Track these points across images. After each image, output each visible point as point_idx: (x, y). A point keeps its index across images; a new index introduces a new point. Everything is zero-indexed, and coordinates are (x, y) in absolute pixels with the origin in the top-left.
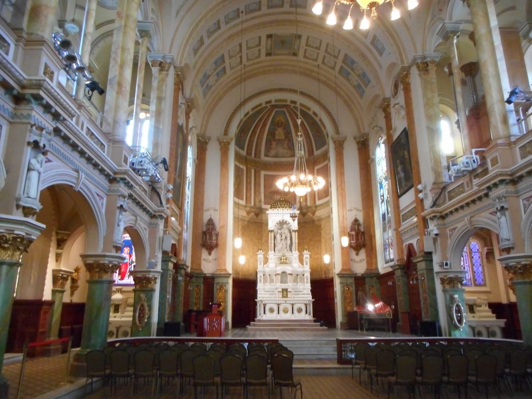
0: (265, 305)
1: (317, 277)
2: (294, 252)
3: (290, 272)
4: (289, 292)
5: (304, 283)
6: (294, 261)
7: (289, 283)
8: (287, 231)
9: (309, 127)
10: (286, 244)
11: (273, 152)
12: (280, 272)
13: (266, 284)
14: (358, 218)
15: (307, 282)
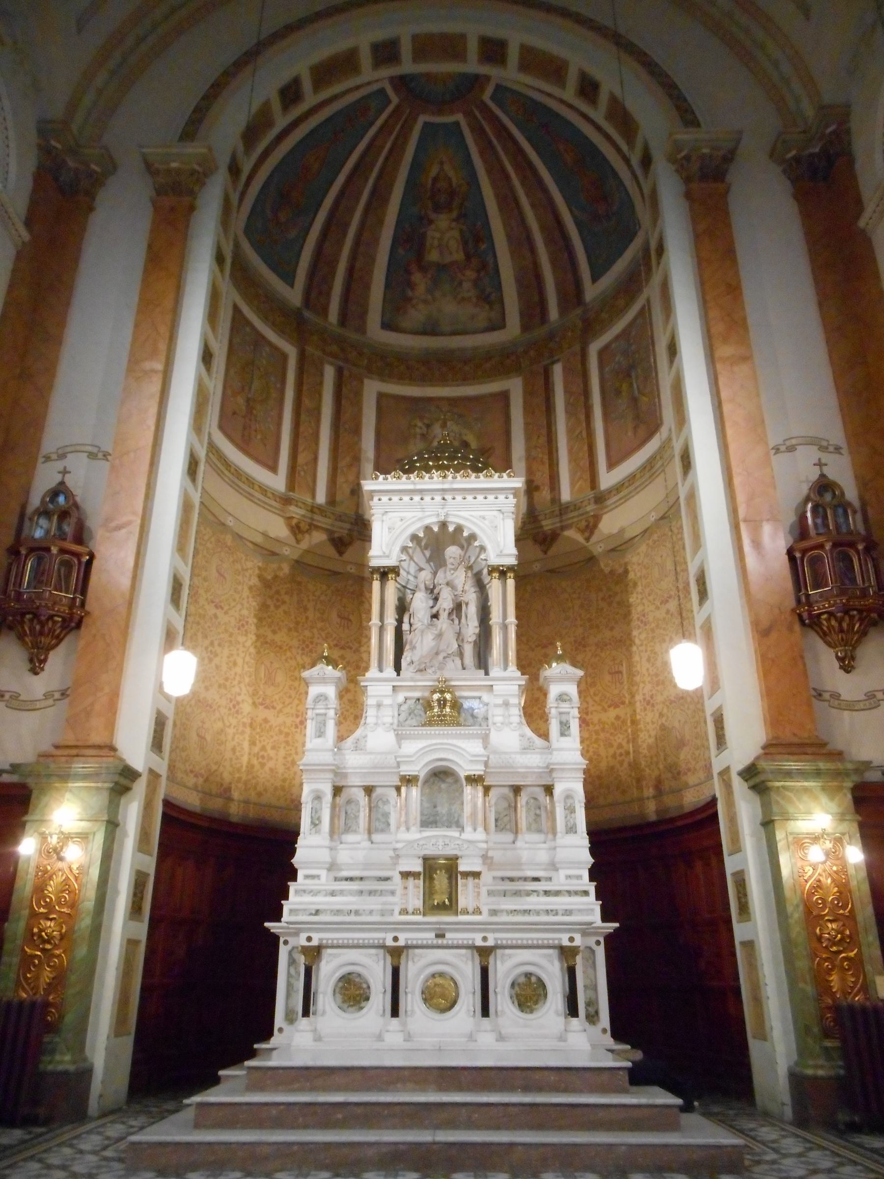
0: (314, 953)
1: (609, 816)
2: (495, 671)
3: (477, 769)
4: (466, 875)
5: (554, 832)
6: (497, 716)
7: (468, 829)
8: (461, 579)
9: (557, 182)
10: (459, 636)
11: (416, 315)
12: (418, 768)
13: (349, 838)
14: (832, 474)
15: (571, 829)
